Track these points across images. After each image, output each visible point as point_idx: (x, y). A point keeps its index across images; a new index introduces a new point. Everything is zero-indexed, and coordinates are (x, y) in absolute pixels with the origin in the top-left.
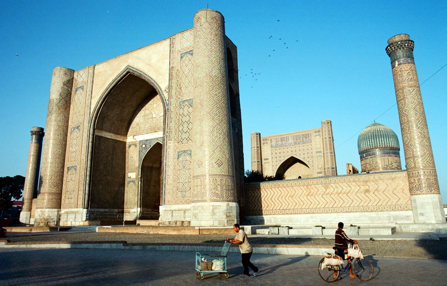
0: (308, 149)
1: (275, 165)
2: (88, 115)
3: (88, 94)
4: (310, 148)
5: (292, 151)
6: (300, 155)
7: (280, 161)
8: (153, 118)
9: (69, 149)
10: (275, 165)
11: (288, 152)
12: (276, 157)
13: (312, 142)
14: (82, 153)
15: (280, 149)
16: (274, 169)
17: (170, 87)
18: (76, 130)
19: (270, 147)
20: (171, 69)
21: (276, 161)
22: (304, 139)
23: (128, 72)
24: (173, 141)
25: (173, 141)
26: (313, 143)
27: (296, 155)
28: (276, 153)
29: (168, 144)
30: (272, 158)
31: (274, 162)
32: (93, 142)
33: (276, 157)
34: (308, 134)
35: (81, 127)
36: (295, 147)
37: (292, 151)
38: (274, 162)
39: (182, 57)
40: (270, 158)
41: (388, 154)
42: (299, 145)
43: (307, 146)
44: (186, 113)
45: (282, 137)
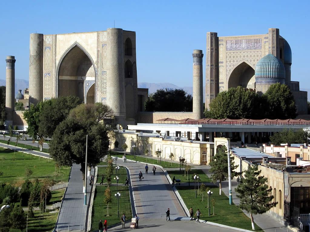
1: (228, 70)
2: (55, 67)
4: (259, 55)
9: (44, 87)
10: (228, 70)
12: (230, 61)
14: (53, 91)
17: (98, 62)
18: (48, 75)
19: (224, 48)
20: (98, 51)
21: (230, 66)
22: (255, 44)
24: (99, 92)
25: (99, 92)
26: (263, 49)
29: (97, 93)
30: (227, 62)
31: (228, 66)
33: (230, 61)
34: (259, 40)
35: (51, 74)
37: (244, 57)
38: (228, 66)
40: (224, 61)
42: (251, 51)
45: (236, 39)
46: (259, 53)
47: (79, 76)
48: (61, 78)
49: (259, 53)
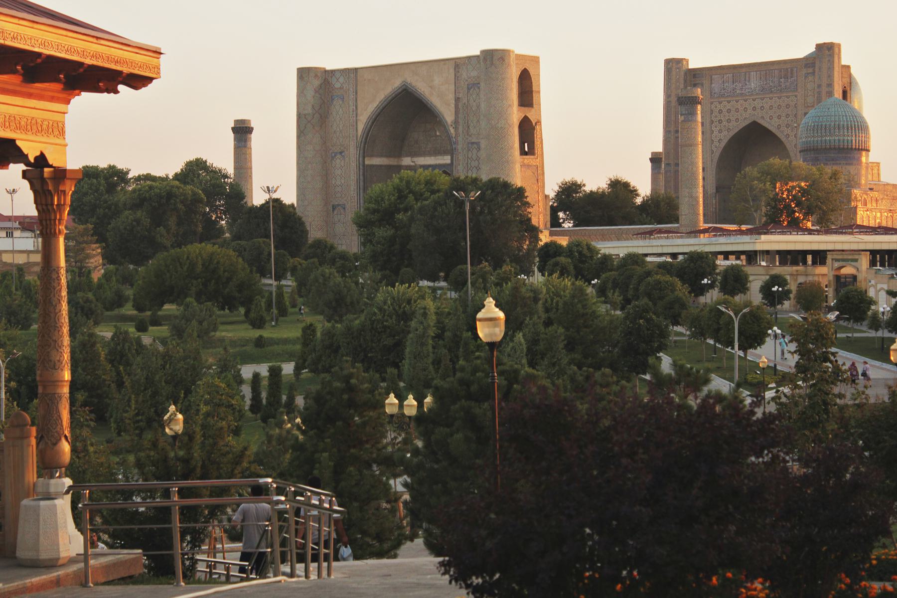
0: (788, 106)
3: (351, 108)
5: (754, 109)
6: (771, 118)
7: (729, 130)
8: (437, 136)
11: (745, 109)
12: (720, 121)
13: (799, 90)
15: (729, 102)
16: (715, 150)
17: (456, 122)
18: (338, 156)
20: (457, 100)
21: (720, 131)
23: (405, 90)
27: (762, 117)
28: (720, 112)
30: (712, 122)
32: (364, 175)
34: (792, 70)
36: (762, 99)
37: (754, 109)
39: (469, 89)
41: (833, 160)
42: (771, 95)
43: (788, 97)
44: (474, 157)
46: (792, 101)
47: (407, 156)
48: (368, 162)
49: (792, 101)
